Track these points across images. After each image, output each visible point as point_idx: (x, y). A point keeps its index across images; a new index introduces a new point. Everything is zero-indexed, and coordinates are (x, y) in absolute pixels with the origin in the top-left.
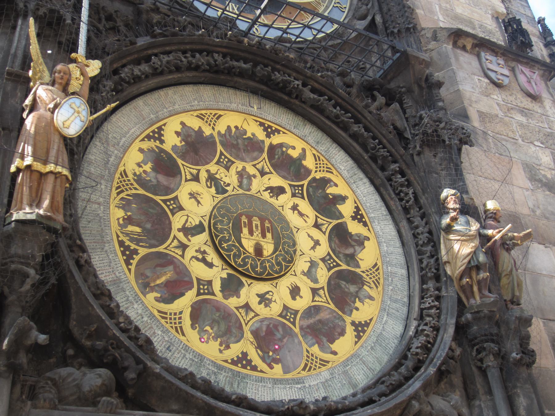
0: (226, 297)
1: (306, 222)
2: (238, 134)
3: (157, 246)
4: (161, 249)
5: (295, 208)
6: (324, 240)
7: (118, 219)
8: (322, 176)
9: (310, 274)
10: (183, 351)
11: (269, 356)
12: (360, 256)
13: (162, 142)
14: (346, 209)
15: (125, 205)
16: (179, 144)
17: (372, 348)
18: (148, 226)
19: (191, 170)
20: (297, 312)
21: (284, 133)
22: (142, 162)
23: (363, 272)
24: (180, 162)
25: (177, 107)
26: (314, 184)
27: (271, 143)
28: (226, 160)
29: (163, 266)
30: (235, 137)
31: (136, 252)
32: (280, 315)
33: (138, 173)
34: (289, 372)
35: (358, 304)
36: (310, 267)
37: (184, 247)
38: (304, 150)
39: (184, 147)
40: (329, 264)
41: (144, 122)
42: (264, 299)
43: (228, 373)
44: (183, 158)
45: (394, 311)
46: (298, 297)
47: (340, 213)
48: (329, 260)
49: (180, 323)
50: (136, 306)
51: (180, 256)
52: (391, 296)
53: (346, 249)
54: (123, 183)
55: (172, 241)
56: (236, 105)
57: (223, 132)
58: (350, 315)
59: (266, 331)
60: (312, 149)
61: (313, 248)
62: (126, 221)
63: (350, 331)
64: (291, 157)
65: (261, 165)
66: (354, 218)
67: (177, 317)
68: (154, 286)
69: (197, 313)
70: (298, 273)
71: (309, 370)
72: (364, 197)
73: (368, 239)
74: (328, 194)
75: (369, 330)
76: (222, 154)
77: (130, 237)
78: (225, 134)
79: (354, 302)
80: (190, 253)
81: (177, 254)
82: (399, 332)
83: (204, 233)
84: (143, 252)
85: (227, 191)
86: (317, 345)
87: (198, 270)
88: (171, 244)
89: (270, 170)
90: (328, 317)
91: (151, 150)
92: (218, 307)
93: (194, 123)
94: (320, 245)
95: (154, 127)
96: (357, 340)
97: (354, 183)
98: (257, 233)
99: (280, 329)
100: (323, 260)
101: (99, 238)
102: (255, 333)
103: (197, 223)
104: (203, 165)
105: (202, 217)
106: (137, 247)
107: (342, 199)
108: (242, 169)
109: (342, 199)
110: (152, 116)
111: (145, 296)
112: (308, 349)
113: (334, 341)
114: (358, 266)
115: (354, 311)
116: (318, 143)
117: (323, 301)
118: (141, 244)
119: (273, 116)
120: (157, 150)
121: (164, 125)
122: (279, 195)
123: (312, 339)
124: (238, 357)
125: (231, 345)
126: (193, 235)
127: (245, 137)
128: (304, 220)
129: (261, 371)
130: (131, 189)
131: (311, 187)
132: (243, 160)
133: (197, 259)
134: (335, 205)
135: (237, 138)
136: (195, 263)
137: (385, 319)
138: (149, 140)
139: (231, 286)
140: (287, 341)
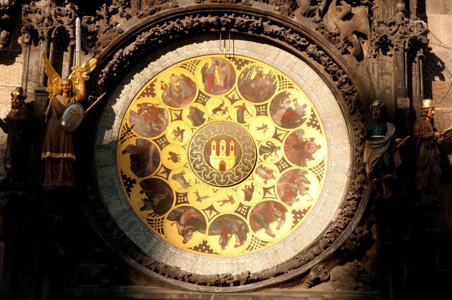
0: (191, 108)
1: (218, 202)
2: (302, 187)
3: (238, 84)
4: (236, 85)
5: (231, 200)
6: (200, 206)
7: (262, 68)
8: (248, 238)
9: (180, 176)
10: (172, 60)
11: (145, 109)
12: (175, 226)
13: (309, 124)
14: (214, 241)
15: (270, 77)
16: (304, 137)
17: (112, 179)
18: (253, 85)
19: (283, 136)
20: (161, 149)
21: (293, 227)
22: (297, 102)
23: (163, 219)
24: (291, 131)
25: (333, 148)
26: (243, 228)
27: (288, 211)
28: (284, 167)
29: (225, 80)
30: (300, 184)
31: (239, 68)
32: (164, 136)
33: (289, 96)
34: (130, 113)
35: (144, 196)
36: (185, 181)
37: (233, 101)
38: (273, 236)
39: (301, 140)
40: (181, 197)
41: (325, 117)
42: (179, 132)
43: (149, 76)
44: (293, 135)
45: (125, 217)
46: (170, 156)
47: (213, 234)
48: (183, 199)
49: (188, 69)
50: (207, 49)
51: (227, 95)
52: (136, 224)
53: (185, 219)
54: (285, 83)
55: (238, 96)
56: (326, 196)
57: (306, 176)
58: (140, 184)
59: (160, 119)
60: (272, 244)
61: (197, 193)
62: (260, 72)
63: (131, 175)
64: (271, 221)
65: (273, 192)
66: (205, 242)
67: (192, 70)
68: (215, 68)
69: (188, 81)
70: (185, 169)
71: (124, 127)
72: (217, 264)
73: (185, 242)
74: (232, 235)
75: (124, 188)
76: (290, 166)
77: (249, 70)
78: (304, 176)
79: (147, 195)
80: (227, 103)
81: (229, 94)
82: (110, 209)
83: (236, 120)
84: (238, 73)
85: (261, 154)
86: (135, 145)
87: (214, 101)
88: (237, 93)
89: (266, 198)
90: (148, 167)
91: (303, 114)
92: (187, 98)
93: (319, 156)
94: (197, 200)
95: (320, 123)
96: (123, 174)
97: (232, 263)
98: (223, 153)
99: (157, 129)
100: (185, 195)
101: (253, 50)
102: (162, 111)
103: (245, 120)
104: (285, 147)
105: (248, 125)
106: (242, 70)
107: (223, 245)
108: (273, 176)
109: (223, 245)
110: (329, 125)
111: (211, 58)
112: (136, 138)
113: (131, 158)
114: (168, 218)
115: (141, 190)
116: (275, 251)
117: (159, 173)
118: (243, 74)
119: (309, 225)
120: (303, 118)
121: (321, 132)
122: (245, 194)
123: (140, 145)
124: (154, 90)
125: (162, 91)
126: (238, 112)
127: (298, 192)
128: (220, 201)
129: (139, 98)
130: (280, 86)
131: (242, 224)
132: (280, 180)
133: (222, 105)
134: (222, 234)
135: (298, 185)
136: (219, 103)
137: (124, 205)
138: (312, 115)
139: (197, 118)
140: (147, 128)
